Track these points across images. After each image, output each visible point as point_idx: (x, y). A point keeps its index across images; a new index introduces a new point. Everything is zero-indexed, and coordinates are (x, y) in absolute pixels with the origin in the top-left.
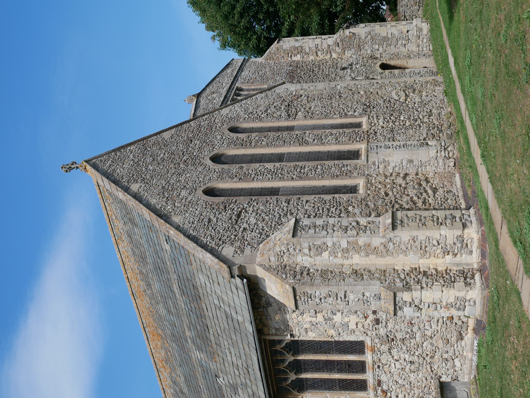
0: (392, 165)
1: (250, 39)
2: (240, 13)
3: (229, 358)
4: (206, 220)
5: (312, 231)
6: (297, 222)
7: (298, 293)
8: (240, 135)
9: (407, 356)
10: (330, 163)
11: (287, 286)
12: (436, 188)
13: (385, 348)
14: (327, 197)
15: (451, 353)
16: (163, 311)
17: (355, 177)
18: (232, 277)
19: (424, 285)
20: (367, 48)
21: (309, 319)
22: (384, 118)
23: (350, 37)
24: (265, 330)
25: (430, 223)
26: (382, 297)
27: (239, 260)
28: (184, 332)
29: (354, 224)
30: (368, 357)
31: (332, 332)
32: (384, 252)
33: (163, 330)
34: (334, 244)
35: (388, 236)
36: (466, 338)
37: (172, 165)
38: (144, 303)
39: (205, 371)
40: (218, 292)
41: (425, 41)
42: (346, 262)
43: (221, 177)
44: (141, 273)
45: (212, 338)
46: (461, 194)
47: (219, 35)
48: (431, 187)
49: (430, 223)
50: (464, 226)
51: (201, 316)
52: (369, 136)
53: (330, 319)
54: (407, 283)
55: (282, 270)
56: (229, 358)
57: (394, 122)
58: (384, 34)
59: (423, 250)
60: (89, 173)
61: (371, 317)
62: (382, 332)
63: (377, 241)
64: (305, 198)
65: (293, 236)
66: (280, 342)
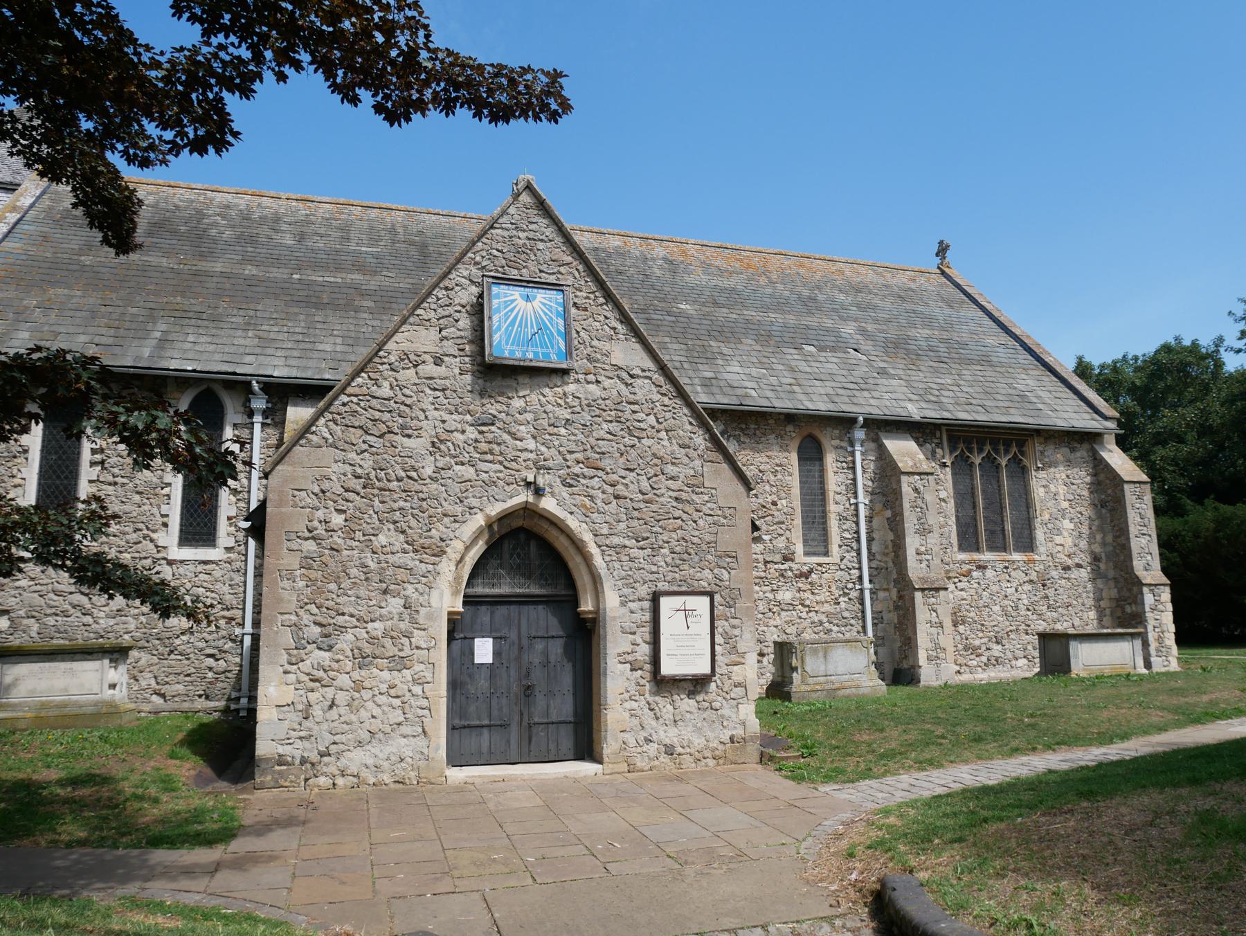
13: (1034, 576)
53: (1063, 517)
61: (1070, 562)
62: (1054, 573)
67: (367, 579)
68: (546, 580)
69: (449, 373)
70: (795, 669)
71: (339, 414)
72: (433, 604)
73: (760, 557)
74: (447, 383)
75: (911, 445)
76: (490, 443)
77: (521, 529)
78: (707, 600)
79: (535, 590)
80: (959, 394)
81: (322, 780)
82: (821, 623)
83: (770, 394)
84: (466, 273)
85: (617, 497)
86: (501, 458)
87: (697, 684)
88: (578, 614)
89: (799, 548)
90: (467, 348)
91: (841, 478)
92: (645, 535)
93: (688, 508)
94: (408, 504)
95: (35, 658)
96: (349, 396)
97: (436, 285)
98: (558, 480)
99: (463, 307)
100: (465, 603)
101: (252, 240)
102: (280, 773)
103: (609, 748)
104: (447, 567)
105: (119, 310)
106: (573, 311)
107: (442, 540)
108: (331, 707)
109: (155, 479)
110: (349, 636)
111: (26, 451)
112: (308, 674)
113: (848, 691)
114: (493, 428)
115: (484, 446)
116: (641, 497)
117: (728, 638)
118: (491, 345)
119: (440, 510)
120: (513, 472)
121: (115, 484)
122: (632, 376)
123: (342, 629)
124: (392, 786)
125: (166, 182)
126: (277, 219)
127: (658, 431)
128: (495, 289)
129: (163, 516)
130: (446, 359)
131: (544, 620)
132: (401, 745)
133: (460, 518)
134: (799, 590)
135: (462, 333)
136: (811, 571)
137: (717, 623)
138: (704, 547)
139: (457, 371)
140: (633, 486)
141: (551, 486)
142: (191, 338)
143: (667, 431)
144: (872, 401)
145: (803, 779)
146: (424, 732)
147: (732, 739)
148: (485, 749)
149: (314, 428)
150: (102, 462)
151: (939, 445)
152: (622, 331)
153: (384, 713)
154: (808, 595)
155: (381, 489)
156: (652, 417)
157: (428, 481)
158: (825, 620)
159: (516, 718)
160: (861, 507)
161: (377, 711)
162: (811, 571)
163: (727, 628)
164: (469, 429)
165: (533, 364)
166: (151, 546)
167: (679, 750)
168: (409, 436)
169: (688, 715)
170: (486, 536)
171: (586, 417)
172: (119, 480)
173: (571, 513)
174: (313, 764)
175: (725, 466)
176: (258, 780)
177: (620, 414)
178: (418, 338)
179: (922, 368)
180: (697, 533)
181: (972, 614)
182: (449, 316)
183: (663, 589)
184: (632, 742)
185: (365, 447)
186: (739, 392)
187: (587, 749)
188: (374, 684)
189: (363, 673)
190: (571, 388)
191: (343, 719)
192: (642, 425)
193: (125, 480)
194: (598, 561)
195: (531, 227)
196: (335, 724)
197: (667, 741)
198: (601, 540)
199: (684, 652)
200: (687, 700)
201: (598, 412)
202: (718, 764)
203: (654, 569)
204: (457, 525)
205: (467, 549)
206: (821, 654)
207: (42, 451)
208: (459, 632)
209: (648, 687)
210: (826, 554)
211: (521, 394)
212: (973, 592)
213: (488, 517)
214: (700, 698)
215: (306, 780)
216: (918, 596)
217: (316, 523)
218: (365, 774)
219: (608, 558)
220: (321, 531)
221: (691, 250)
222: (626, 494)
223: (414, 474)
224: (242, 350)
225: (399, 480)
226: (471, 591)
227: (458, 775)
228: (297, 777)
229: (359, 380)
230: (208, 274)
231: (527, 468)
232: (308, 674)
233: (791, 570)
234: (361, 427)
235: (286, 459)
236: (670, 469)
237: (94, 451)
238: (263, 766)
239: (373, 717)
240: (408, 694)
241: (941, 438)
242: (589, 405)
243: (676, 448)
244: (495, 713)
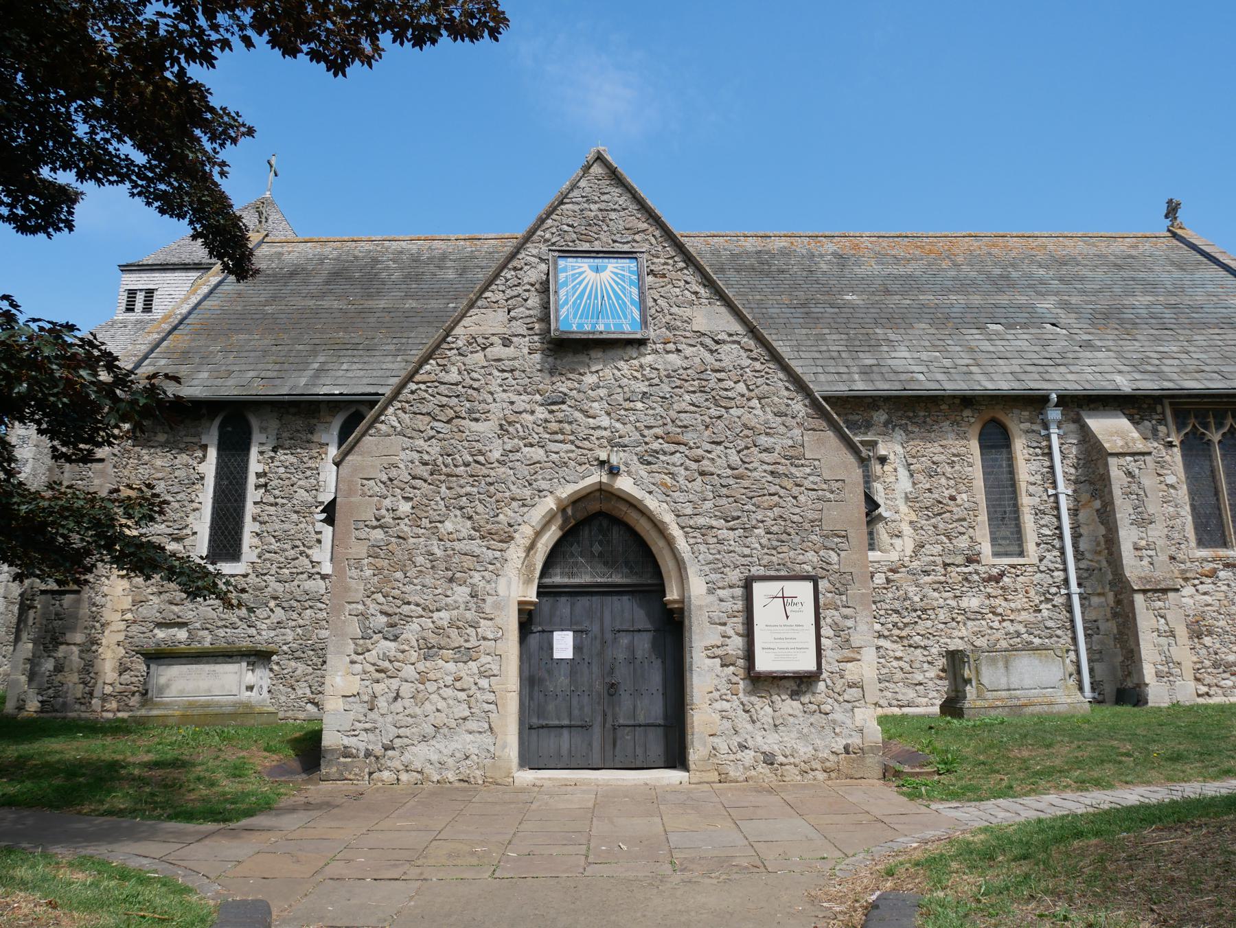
67: (433, 567)
68: (631, 568)
69: (518, 354)
70: (969, 681)
71: (407, 402)
72: (501, 592)
73: (939, 560)
74: (516, 363)
75: (1123, 423)
76: (560, 422)
77: (600, 514)
78: (809, 586)
79: (617, 579)
80: (1186, 362)
81: (386, 775)
82: (1018, 635)
83: (940, 377)
84: (535, 252)
85: (702, 474)
86: (572, 438)
87: (801, 683)
88: (665, 604)
89: (986, 548)
90: (537, 326)
91: (1035, 466)
92: (735, 514)
93: (788, 483)
94: (475, 490)
95: (183, 660)
96: (417, 383)
97: (504, 267)
98: (635, 458)
99: (532, 285)
100: (539, 594)
101: (418, 278)
102: (345, 764)
103: (695, 754)
104: (515, 553)
105: (287, 348)
106: (650, 279)
107: (510, 525)
108: (396, 699)
109: (310, 499)
110: (415, 626)
111: (202, 478)
112: (374, 665)
113: (1038, 709)
114: (564, 407)
115: (554, 426)
116: (730, 472)
117: (838, 630)
118: (557, 320)
119: (507, 494)
120: (585, 452)
121: (276, 504)
122: (717, 342)
123: (408, 618)
124: (457, 784)
125: (351, 237)
126: (444, 257)
127: (749, 400)
128: (562, 263)
129: (317, 533)
130: (514, 339)
131: (628, 611)
132: (465, 742)
133: (528, 502)
134: (989, 596)
135: (531, 312)
136: (1002, 574)
137: (823, 613)
138: (807, 526)
139: (526, 351)
140: (721, 460)
141: (627, 465)
142: (345, 367)
143: (759, 399)
144: (1070, 377)
145: (920, 796)
146: (491, 728)
147: (847, 749)
148: (564, 751)
149: (383, 418)
150: (265, 485)
151: (1162, 421)
152: (704, 295)
153: (449, 707)
154: (1000, 601)
155: (448, 475)
156: (741, 385)
157: (496, 464)
158: (1023, 630)
159: (599, 719)
160: (1062, 498)
161: (441, 705)
162: (1002, 574)
163: (838, 618)
164: (539, 409)
165: (604, 336)
166: (307, 561)
167: (781, 759)
168: (477, 420)
169: (791, 719)
170: (559, 521)
171: (666, 388)
172: (279, 501)
173: (650, 493)
174: (377, 758)
175: (830, 433)
176: (323, 771)
177: (704, 383)
178: (487, 321)
179: (1139, 337)
180: (797, 510)
181: (1222, 623)
182: (519, 296)
183: (756, 574)
184: (724, 748)
185: (433, 433)
186: (903, 377)
187: (676, 758)
188: (439, 675)
189: (428, 664)
190: (649, 359)
191: (407, 712)
192: (730, 394)
193: (284, 501)
194: (682, 544)
195: (603, 198)
196: (400, 717)
197: (766, 748)
198: (684, 521)
199: (784, 641)
200: (789, 701)
201: (678, 383)
202: (830, 778)
203: (747, 551)
204: (526, 509)
205: (538, 534)
206: (1001, 664)
207: (216, 477)
208: (528, 620)
209: (742, 685)
210: (1021, 554)
211: (594, 369)
212: (1221, 596)
213: (559, 500)
214: (805, 699)
215: (370, 774)
216: (1139, 599)
217: (383, 512)
218: (429, 770)
219: (692, 541)
220: (388, 519)
221: (866, 242)
222: (712, 470)
223: (481, 459)
224: (388, 373)
225: (467, 465)
226: (547, 581)
227: (528, 776)
228: (362, 770)
229: (428, 367)
230: (371, 311)
231: (601, 446)
232: (374, 665)
233: (977, 573)
234: (429, 414)
235: (356, 449)
236: (764, 440)
237: (258, 475)
238: (329, 757)
239: (438, 710)
240: (474, 688)
241: (1163, 413)
242: (668, 376)
243: (770, 416)
244: (576, 712)
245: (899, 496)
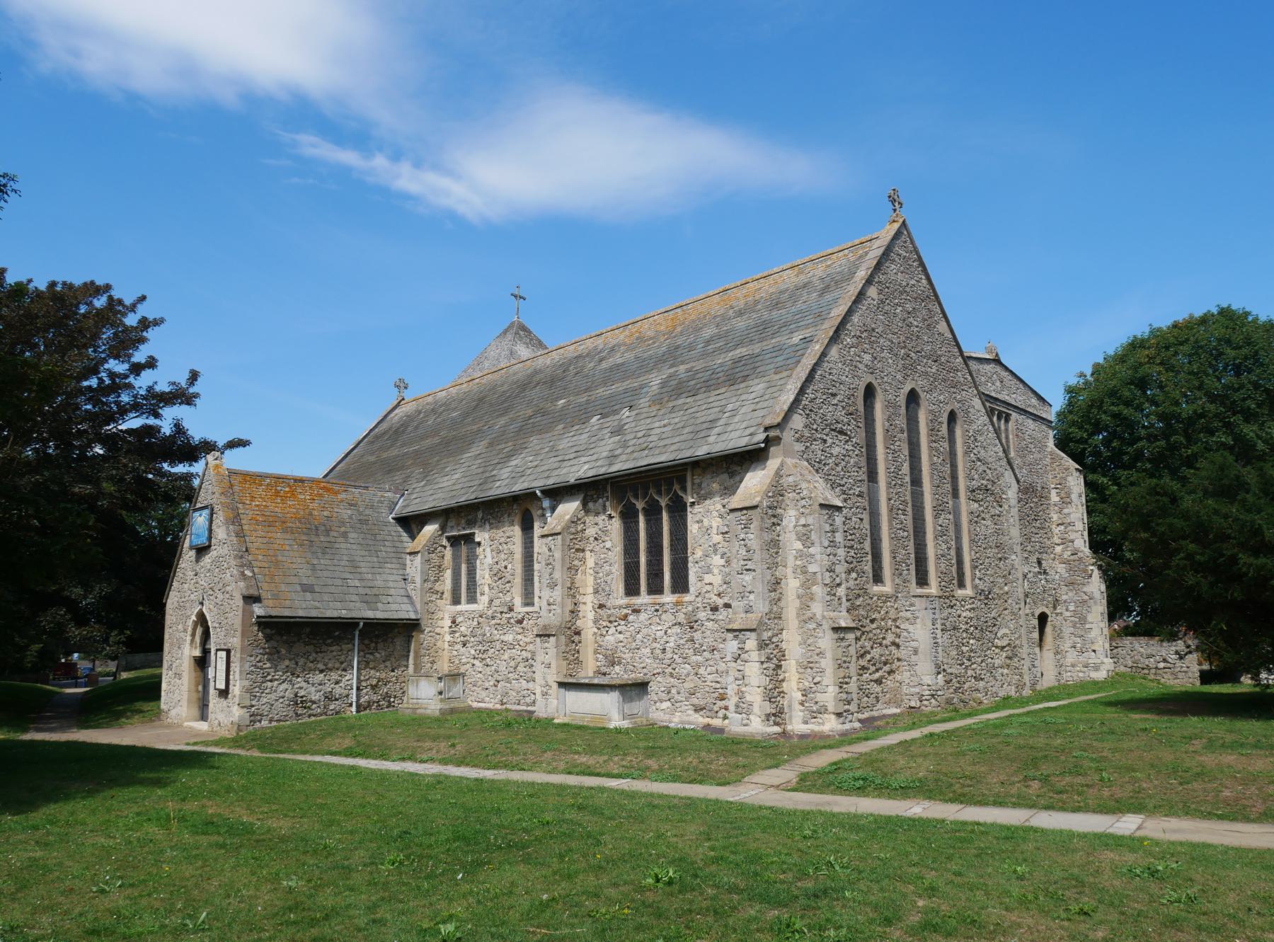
0: (911, 628)
1: (1080, 428)
2: (1120, 414)
3: (657, 424)
4: (834, 390)
5: (828, 528)
6: (839, 509)
7: (750, 512)
8: (945, 426)
9: (672, 644)
10: (911, 549)
11: (758, 499)
12: (881, 683)
13: (681, 618)
14: (867, 545)
15: (678, 697)
16: (708, 332)
17: (893, 581)
18: (766, 429)
19: (765, 666)
20: (1070, 594)
21: (714, 525)
22: (971, 618)
23: (1085, 571)
24: (699, 471)
25: (841, 673)
26: (749, 615)
27: (787, 436)
28: (683, 363)
29: (838, 580)
30: (668, 598)
31: (699, 554)
32: (805, 617)
33: (682, 333)
34: (812, 556)
35: (824, 622)
36: (697, 715)
37: (903, 339)
38: (715, 307)
39: (636, 392)
40: (743, 410)
41: (1081, 675)
42: (789, 571)
43: (889, 405)
44: (756, 302)
45: (680, 401)
46: (875, 714)
47: (1086, 382)
48: (883, 677)
49: (841, 673)
50: (839, 715)
51: (709, 386)
52: (947, 598)
53: (715, 551)
54: (767, 645)
55: (777, 491)
56: (657, 424)
57: (966, 631)
58: (1090, 619)
59: (807, 666)
60: (888, 227)
61: (720, 602)
62: (702, 615)
63: (817, 608)
64: (866, 516)
65: (821, 505)
66: (684, 489)
245: (486, 566)
